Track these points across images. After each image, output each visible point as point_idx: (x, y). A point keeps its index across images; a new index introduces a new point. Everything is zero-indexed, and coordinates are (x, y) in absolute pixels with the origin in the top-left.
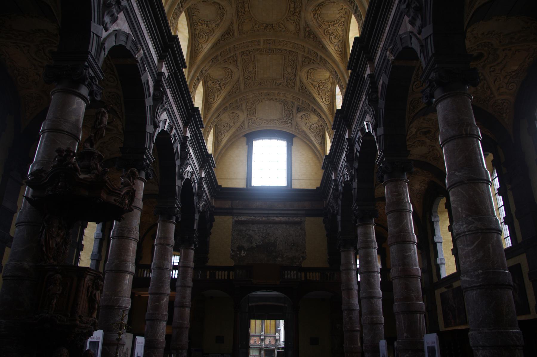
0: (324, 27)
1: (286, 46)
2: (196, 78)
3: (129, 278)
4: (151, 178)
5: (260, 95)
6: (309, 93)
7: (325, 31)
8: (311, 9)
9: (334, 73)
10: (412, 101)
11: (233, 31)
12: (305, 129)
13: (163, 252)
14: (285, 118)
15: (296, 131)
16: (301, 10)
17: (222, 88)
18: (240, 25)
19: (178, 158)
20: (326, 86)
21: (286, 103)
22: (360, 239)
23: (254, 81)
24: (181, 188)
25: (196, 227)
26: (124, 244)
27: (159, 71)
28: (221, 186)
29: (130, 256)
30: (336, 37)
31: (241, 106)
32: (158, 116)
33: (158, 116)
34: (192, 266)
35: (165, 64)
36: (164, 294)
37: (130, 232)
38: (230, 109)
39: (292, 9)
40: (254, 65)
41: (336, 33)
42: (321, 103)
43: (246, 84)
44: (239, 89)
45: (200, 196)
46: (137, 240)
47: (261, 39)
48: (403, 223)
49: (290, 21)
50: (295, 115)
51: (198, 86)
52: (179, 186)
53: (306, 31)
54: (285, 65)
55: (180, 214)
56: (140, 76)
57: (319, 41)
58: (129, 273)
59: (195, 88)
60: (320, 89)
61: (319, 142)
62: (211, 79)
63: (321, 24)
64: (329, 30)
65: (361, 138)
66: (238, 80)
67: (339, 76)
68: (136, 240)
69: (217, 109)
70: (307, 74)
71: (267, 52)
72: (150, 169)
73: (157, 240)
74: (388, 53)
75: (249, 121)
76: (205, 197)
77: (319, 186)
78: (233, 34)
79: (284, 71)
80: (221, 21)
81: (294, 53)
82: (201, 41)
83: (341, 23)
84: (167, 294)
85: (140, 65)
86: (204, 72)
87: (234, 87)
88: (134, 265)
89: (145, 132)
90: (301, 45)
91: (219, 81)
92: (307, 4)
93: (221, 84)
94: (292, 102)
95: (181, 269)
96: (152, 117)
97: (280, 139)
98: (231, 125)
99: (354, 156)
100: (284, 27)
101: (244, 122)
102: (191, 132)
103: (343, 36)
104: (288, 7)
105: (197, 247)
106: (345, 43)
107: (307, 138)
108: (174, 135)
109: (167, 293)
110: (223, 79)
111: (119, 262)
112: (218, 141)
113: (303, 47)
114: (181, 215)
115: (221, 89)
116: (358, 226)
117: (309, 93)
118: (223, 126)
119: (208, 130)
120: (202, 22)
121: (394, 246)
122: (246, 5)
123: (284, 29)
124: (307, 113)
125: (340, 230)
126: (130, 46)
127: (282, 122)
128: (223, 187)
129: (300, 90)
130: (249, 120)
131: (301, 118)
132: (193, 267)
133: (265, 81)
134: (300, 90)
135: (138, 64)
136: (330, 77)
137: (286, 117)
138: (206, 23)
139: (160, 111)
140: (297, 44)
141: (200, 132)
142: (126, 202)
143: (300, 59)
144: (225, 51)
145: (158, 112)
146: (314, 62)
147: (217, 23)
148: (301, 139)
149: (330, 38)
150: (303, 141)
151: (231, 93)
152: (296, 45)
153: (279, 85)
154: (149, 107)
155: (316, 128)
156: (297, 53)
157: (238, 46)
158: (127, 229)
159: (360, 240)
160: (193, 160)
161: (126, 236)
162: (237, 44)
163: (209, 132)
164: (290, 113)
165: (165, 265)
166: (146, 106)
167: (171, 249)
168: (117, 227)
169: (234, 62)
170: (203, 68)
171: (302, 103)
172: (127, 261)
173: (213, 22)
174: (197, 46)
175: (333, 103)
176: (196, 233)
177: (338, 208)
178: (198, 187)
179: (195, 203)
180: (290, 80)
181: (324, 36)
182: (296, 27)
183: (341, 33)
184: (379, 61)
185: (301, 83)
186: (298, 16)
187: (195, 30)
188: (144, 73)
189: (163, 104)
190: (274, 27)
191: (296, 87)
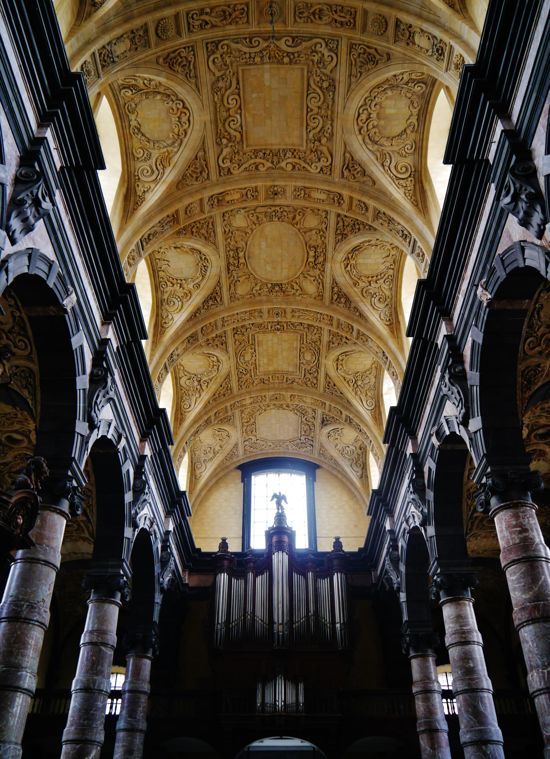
0: (362, 284)
1: (302, 317)
2: (162, 366)
3: (22, 703)
4: (79, 513)
5: (262, 399)
6: (341, 393)
7: (364, 291)
8: (340, 256)
9: (380, 355)
10: (524, 371)
11: (221, 294)
12: (334, 453)
13: (94, 658)
14: (303, 438)
15: (320, 458)
16: (325, 260)
17: (203, 388)
18: (231, 285)
19: (130, 490)
20: (365, 382)
21: (304, 412)
22: (449, 627)
23: (253, 377)
24: (132, 542)
25: (156, 618)
26: (19, 633)
27: (103, 337)
28: (199, 550)
29: (29, 656)
30: (381, 300)
31: (232, 417)
32: (96, 408)
33: (96, 408)
34: (146, 690)
35: (112, 327)
36: (92, 742)
37: (33, 610)
38: (216, 422)
39: (311, 259)
40: (253, 350)
41: (381, 294)
42: (360, 408)
43: (240, 382)
44: (230, 389)
45: (164, 563)
46: (45, 626)
47: (265, 307)
48: (540, 583)
49: (309, 277)
50: (318, 431)
51: (165, 378)
52: (129, 539)
53: (334, 292)
54: (302, 350)
55: (129, 588)
56: (70, 338)
57: (355, 307)
58: (24, 691)
59: (161, 380)
60: (357, 385)
61: (359, 474)
62: (185, 373)
63: (357, 279)
64: (370, 289)
65: (437, 447)
66: (229, 375)
67: (389, 358)
68: (42, 626)
69: (195, 421)
70: (336, 362)
71: (273, 328)
72: (79, 496)
73: (85, 636)
74: (480, 289)
75: (245, 443)
76: (173, 566)
77: (362, 546)
78: (221, 300)
79: (300, 360)
80: (202, 279)
81: (315, 330)
82: (171, 309)
83: (388, 278)
84: (98, 742)
85: (70, 318)
86: (175, 357)
87: (221, 386)
88: (34, 676)
89: (74, 432)
90: (327, 315)
91: (199, 376)
92: (335, 248)
93: (202, 381)
94: (314, 410)
95: (127, 695)
96: (87, 408)
97: (295, 473)
98: (216, 449)
99: (426, 481)
100: (299, 288)
101: (236, 445)
102: (153, 449)
103: (392, 297)
104: (306, 256)
105: (157, 653)
106: (395, 308)
107: (339, 469)
108: (124, 448)
109: (98, 740)
110: (205, 374)
111: (4, 669)
112: (195, 476)
113: (329, 318)
114: (130, 591)
115: (202, 389)
116: (444, 603)
117: (341, 393)
118: (203, 451)
119: (180, 454)
120: (172, 281)
121: (527, 628)
122: (241, 254)
123: (299, 292)
124: (337, 426)
125: (405, 618)
126: (54, 283)
127: (297, 445)
128: (203, 550)
129: (327, 389)
130: (244, 442)
131: (328, 436)
132: (149, 692)
133: (271, 377)
134: (327, 389)
135: (66, 316)
136: (373, 366)
137: (304, 435)
138: (179, 281)
139: (101, 401)
140: (321, 314)
141: (167, 452)
142: (19, 521)
143: (326, 338)
144: (208, 325)
145: (98, 401)
146: (347, 341)
147: (197, 281)
148: (328, 471)
149: (371, 302)
150: (332, 474)
151: (217, 395)
152: (319, 315)
153: (292, 383)
154: (81, 391)
155: (352, 452)
156: (320, 329)
157: (229, 318)
158: (27, 603)
159: (451, 630)
160: (153, 498)
161: (23, 616)
162: (227, 314)
163: (181, 457)
164: (310, 429)
165: (97, 684)
166: (78, 388)
167: (110, 653)
168: (10, 599)
169: (222, 345)
170: (174, 351)
171: (330, 411)
172: (22, 668)
173: (190, 280)
174: (164, 317)
175: (379, 407)
176: (156, 627)
177: (399, 579)
178: (162, 546)
179: (156, 574)
180: (310, 374)
181: (362, 298)
182: (318, 288)
183: (388, 293)
184: (462, 312)
185: (328, 378)
186: (322, 269)
187: (163, 293)
188: (77, 333)
189: (106, 389)
190: (283, 289)
191: (319, 384)
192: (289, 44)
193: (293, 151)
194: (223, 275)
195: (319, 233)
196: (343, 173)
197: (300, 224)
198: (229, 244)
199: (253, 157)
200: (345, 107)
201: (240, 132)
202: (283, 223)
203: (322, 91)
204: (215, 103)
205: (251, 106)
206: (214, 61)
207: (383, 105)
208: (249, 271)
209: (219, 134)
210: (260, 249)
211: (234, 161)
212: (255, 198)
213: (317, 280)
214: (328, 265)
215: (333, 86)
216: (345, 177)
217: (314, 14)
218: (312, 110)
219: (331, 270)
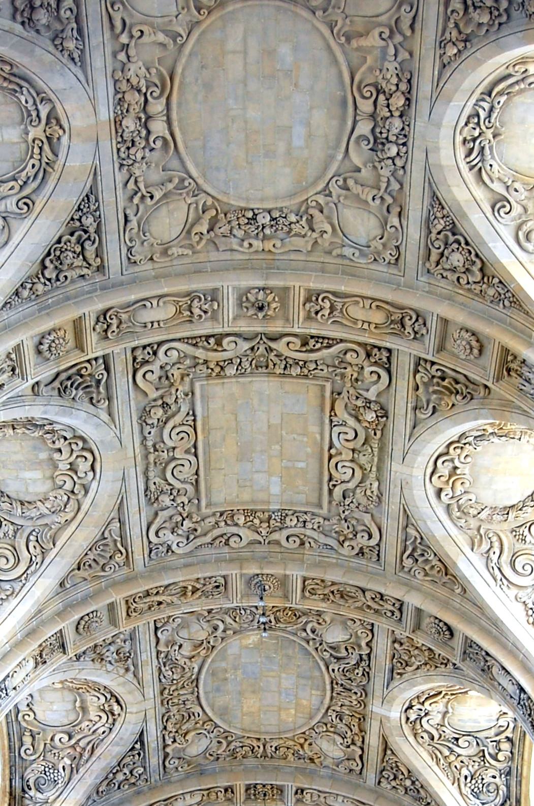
16: (117, 123)
18: (408, 33)
39: (157, 107)
92: (95, 174)
104: (174, 116)
122: (364, 128)
192: (237, 539)
193: (222, 373)
194: (424, 87)
195: (143, 197)
196: (107, 369)
197: (197, 208)
198: (393, 174)
199: (313, 366)
201: (336, 415)
202: (243, 204)
203: (170, 484)
205: (309, 450)
206: (370, 537)
207: (48, 485)
208: (345, 53)
209: (380, 428)
210: (308, 124)
211: (356, 369)
212: (312, 296)
213: (132, 37)
214: (105, 113)
215: (151, 497)
216: (101, 361)
218: (187, 452)
219: (93, 101)
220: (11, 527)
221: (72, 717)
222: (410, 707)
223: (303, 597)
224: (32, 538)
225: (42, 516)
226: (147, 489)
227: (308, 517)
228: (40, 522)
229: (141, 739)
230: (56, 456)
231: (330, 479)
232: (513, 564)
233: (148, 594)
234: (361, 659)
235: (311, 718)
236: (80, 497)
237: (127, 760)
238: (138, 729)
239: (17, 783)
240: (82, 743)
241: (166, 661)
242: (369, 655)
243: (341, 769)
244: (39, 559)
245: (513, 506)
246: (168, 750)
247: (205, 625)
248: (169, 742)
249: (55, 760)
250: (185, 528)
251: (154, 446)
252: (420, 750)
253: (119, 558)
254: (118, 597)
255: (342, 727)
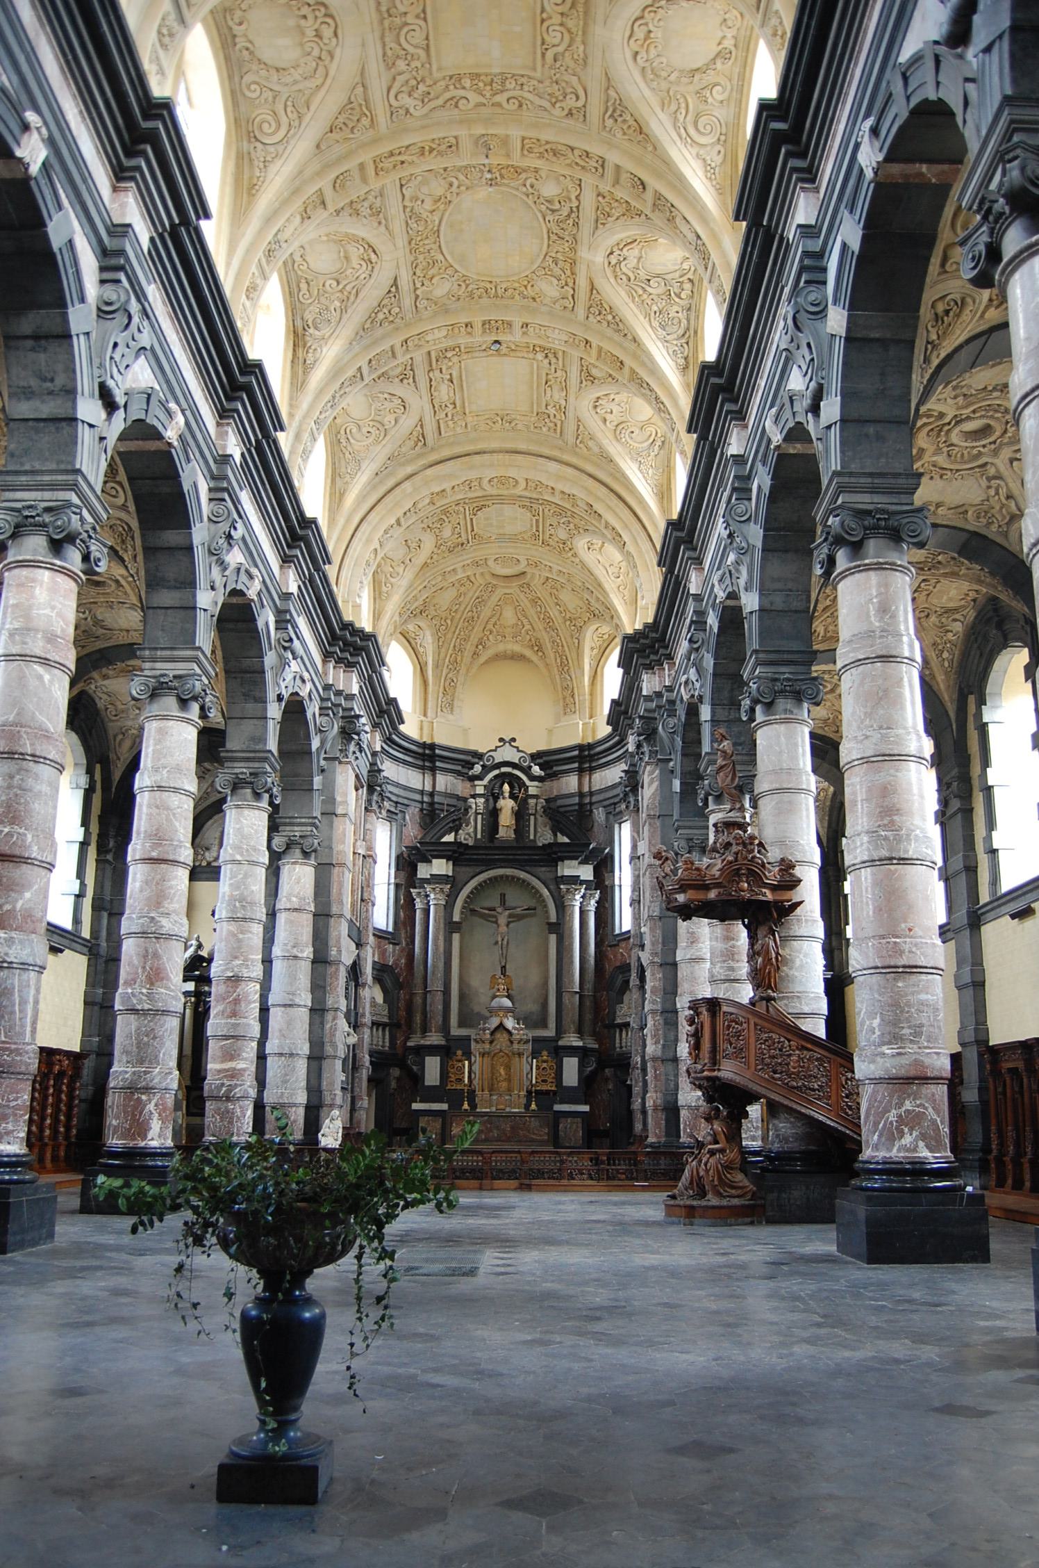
192: (464, 101)
200: (363, 45)
204: (584, 43)
206: (578, 98)
217: (431, 150)
218: (417, 17)
220: (270, 94)
221: (338, 266)
222: (611, 253)
223: (523, 155)
224: (289, 103)
225: (295, 82)
226: (384, 55)
227: (524, 80)
228: (296, 88)
229: (395, 284)
230: (303, 22)
231: (543, 43)
232: (696, 124)
233: (391, 154)
234: (572, 211)
235: (532, 263)
236: (326, 63)
237: (386, 301)
238: (392, 276)
239: (299, 323)
240: (348, 288)
241: (412, 216)
242: (578, 207)
243: (557, 306)
244: (296, 123)
245: (697, 70)
246: (418, 292)
247: (442, 182)
248: (418, 285)
249: (327, 303)
250: (420, 91)
251: (388, 11)
252: (620, 290)
253: (365, 122)
254: (366, 157)
255: (557, 271)
